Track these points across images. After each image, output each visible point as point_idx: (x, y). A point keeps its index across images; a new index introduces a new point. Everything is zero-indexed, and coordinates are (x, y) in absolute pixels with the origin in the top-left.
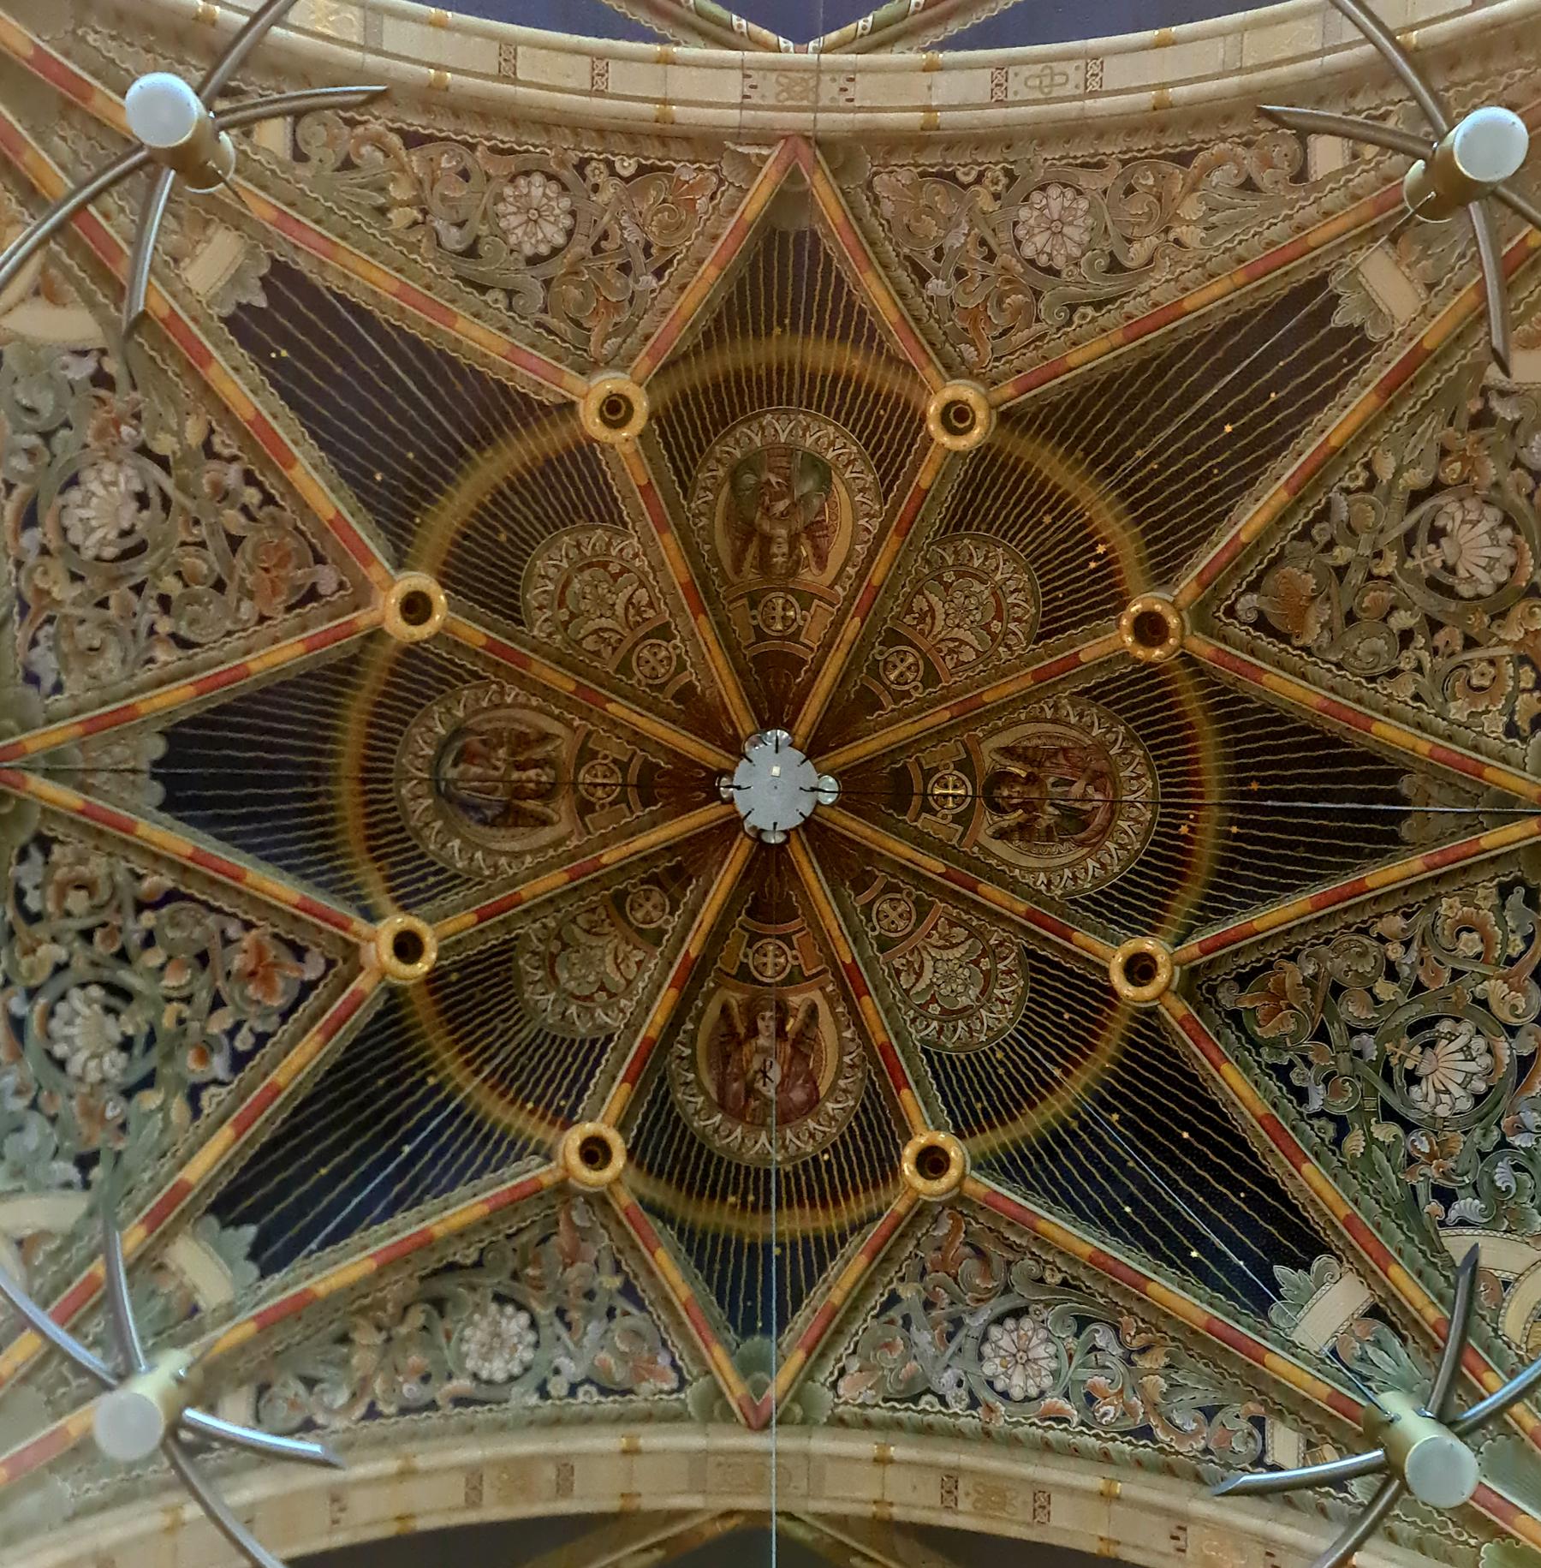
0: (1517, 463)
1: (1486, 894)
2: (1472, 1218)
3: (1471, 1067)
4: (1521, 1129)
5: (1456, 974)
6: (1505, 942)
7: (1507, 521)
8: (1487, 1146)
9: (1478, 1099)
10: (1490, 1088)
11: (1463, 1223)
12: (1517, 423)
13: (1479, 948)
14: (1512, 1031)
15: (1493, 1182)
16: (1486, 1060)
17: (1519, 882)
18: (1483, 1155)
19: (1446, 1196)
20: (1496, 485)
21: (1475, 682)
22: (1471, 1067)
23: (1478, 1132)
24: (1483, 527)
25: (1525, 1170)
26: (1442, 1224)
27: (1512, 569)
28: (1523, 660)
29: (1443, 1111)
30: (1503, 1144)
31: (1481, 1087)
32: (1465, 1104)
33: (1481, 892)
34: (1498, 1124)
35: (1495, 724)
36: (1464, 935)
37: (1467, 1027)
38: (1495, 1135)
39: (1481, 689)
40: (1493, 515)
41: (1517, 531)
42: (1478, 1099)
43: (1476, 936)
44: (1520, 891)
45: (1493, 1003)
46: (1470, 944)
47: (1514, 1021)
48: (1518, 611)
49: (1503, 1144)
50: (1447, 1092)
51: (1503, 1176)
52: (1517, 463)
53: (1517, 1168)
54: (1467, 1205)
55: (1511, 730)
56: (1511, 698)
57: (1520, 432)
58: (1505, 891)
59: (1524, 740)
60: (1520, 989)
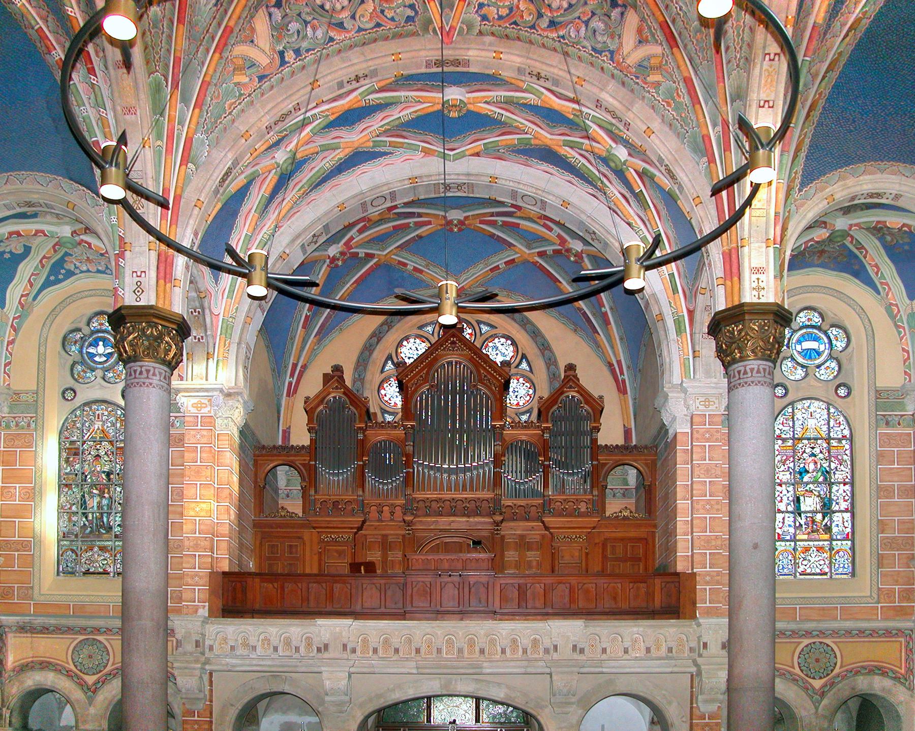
0: (593, 14)
2: (273, 17)
4: (314, 29)
6: (390, 9)
8: (303, 15)
11: (270, 15)
12: (609, 17)
17: (417, 13)
18: (299, 15)
27: (549, 6)
30: (306, 23)
34: (314, 19)
45: (363, 6)
47: (357, 17)
49: (306, 23)
53: (298, 32)
54: (277, 14)
59: (477, 12)
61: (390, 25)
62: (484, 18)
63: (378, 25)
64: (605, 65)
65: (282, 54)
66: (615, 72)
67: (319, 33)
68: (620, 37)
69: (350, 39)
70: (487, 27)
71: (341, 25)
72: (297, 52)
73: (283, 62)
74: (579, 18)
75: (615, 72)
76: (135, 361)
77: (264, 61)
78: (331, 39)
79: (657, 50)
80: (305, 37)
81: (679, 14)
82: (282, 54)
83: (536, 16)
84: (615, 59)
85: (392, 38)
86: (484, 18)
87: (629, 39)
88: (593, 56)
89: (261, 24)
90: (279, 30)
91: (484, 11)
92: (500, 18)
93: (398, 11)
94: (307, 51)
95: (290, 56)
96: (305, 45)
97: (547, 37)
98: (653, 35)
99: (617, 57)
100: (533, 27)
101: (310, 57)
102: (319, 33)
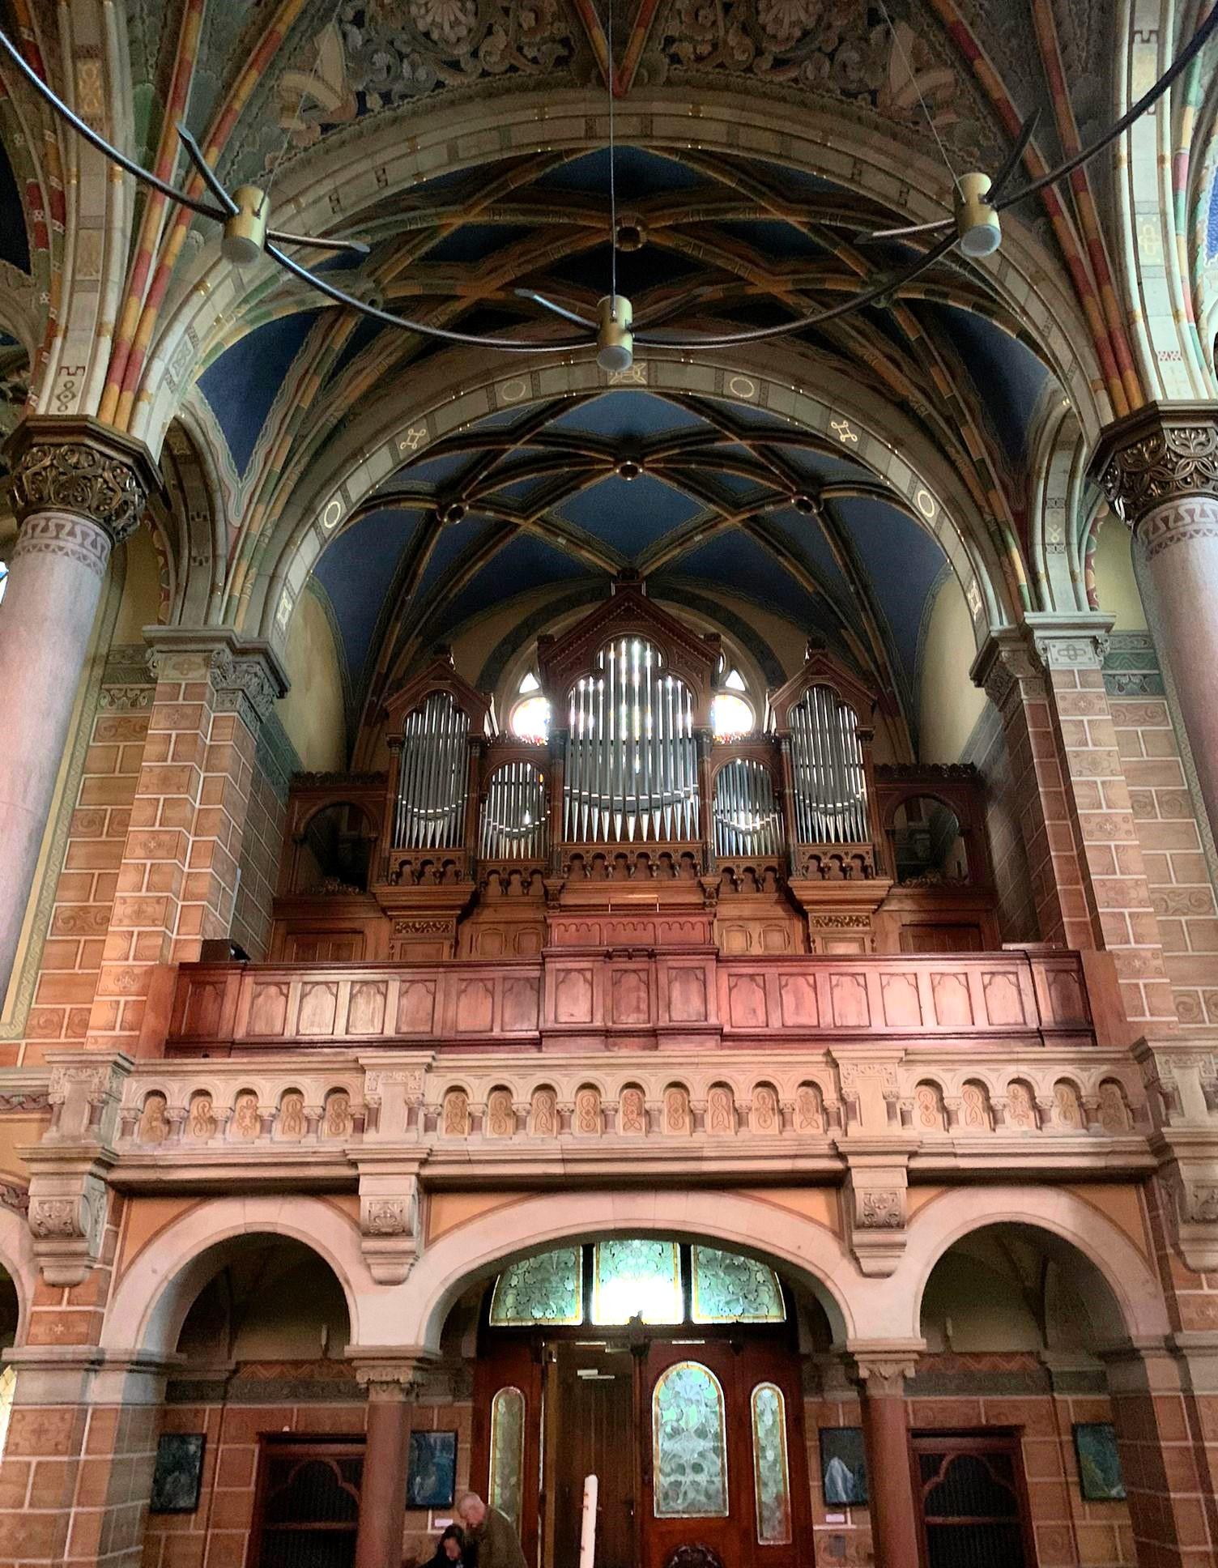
0: (841, 40)
1: (561, 29)
2: (350, 39)
3: (447, 27)
4: (414, 67)
5: (506, 11)
6: (530, 45)
7: (806, 33)
8: (397, 44)
9: (427, 35)
10: (435, 43)
11: (345, 36)
12: (867, 40)
13: (525, 27)
14: (475, 54)
15: (376, 51)
16: (453, 38)
17: (571, 50)
18: (392, 43)
19: (359, 20)
20: (829, 26)
21: (702, 13)
22: (447, 27)
23: (405, 37)
24: (803, 16)
25: (389, 71)
26: (340, 21)
27: (774, 37)
28: (715, 46)
29: (414, 9)
30: (401, 57)
31: (435, 36)
32: (422, 26)
33: (563, 25)
34: (413, 50)
35: (673, 29)
36: (532, 15)
37: (471, 21)
38: (406, 50)
39: (697, 16)
40: (810, 23)
41: (799, 41)
42: (427, 35)
43: (533, 23)
44: (564, 52)
45: (490, 39)
46: (528, 20)
47: (481, 54)
48: (748, 41)
49: (401, 57)
50: (427, 11)
51: (382, 59)
52: (841, 40)
53: (389, 68)
54: (357, 36)
55: (670, 41)
56: (691, 40)
57: (863, 45)
58: (565, 42)
59: (663, 50)
60: (503, 58)
61: (530, 69)
62: (675, 59)
63: (513, 68)
64: (863, 113)
65: (361, 97)
66: (880, 120)
67: (422, 74)
68: (884, 70)
69: (469, 86)
70: (678, 72)
71: (455, 66)
72: (386, 98)
73: (363, 109)
74: (820, 49)
75: (880, 120)
76: (36, 512)
77: (332, 103)
78: (440, 84)
79: (944, 76)
80: (399, 77)
81: (978, 15)
82: (361, 97)
83: (753, 53)
84: (879, 101)
85: (534, 89)
86: (675, 59)
87: (900, 65)
88: (841, 101)
89: (329, 46)
90: (358, 61)
91: (673, 49)
92: (699, 59)
93: (544, 48)
94: (403, 97)
95: (374, 101)
96: (398, 88)
97: (771, 82)
98: (938, 55)
99: (880, 98)
100: (749, 69)
101: (406, 107)
102: (422, 74)
